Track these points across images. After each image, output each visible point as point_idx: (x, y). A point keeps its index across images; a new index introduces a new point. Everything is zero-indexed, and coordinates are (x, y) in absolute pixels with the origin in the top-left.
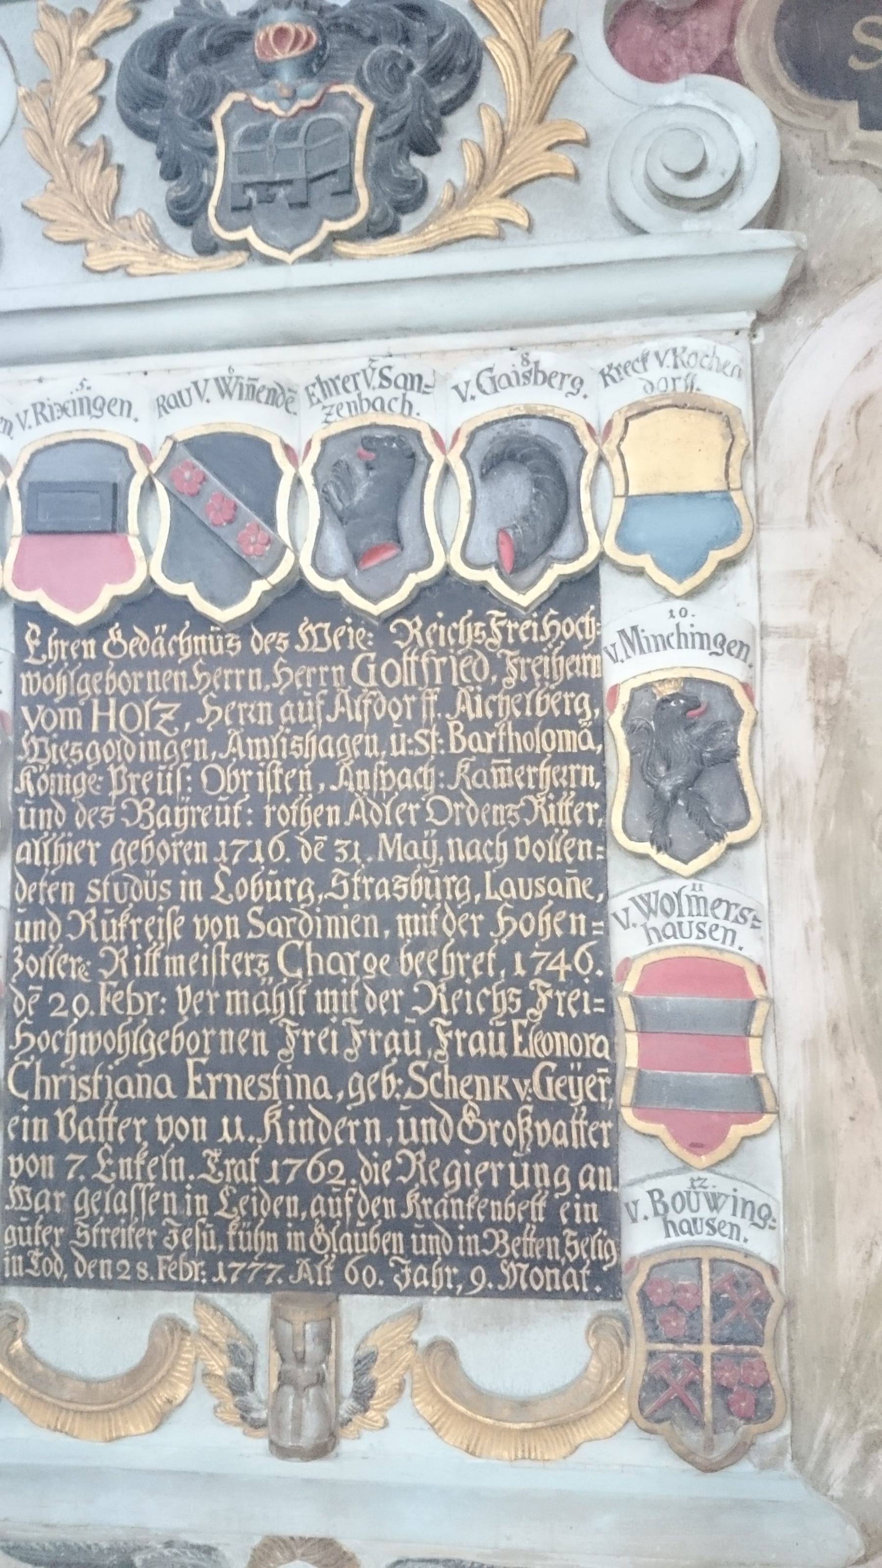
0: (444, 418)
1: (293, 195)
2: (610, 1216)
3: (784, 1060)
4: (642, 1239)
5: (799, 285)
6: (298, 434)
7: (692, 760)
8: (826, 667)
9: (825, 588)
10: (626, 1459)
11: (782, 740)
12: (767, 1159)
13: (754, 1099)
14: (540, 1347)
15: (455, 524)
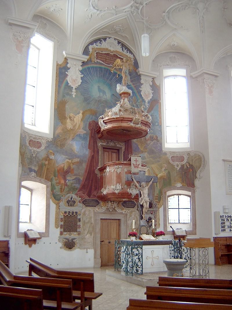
0: (74, 211)
1: (71, 205)
2: (77, 230)
3: (81, 227)
4: (78, 231)
5: (83, 209)
6: (71, 211)
7: (80, 220)
8: (82, 218)
9: (82, 216)
10: (77, 236)
11: (81, 220)
12: (81, 229)
13: (80, 227)
14: (76, 233)
15: (74, 213)
